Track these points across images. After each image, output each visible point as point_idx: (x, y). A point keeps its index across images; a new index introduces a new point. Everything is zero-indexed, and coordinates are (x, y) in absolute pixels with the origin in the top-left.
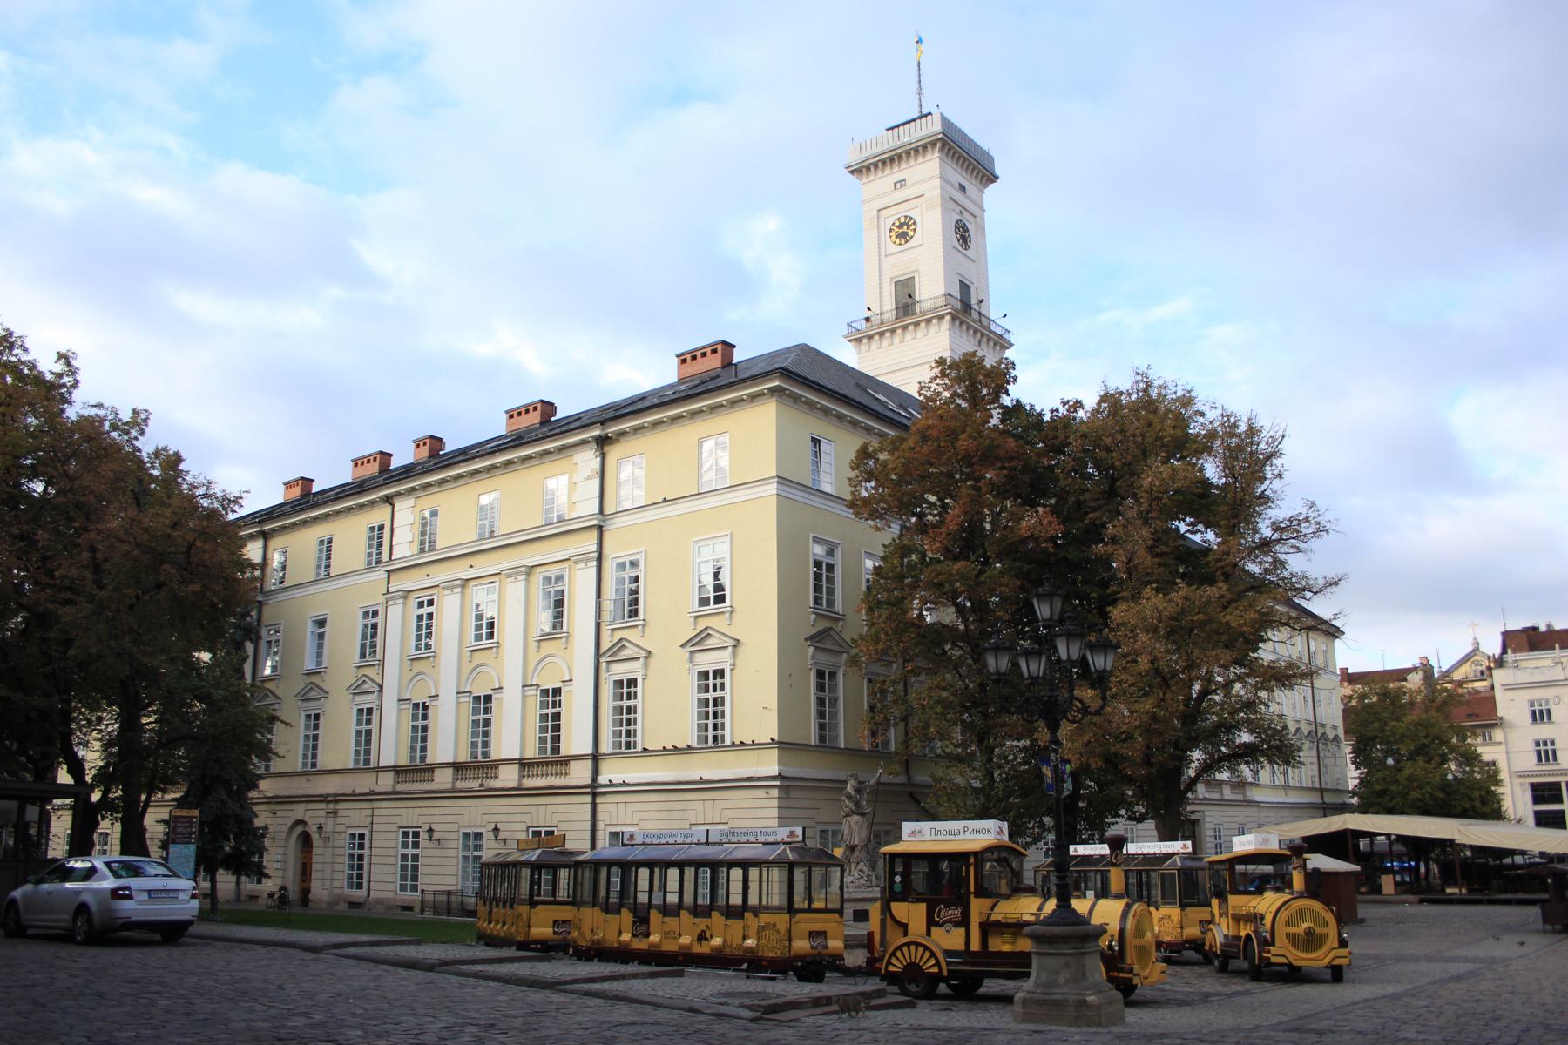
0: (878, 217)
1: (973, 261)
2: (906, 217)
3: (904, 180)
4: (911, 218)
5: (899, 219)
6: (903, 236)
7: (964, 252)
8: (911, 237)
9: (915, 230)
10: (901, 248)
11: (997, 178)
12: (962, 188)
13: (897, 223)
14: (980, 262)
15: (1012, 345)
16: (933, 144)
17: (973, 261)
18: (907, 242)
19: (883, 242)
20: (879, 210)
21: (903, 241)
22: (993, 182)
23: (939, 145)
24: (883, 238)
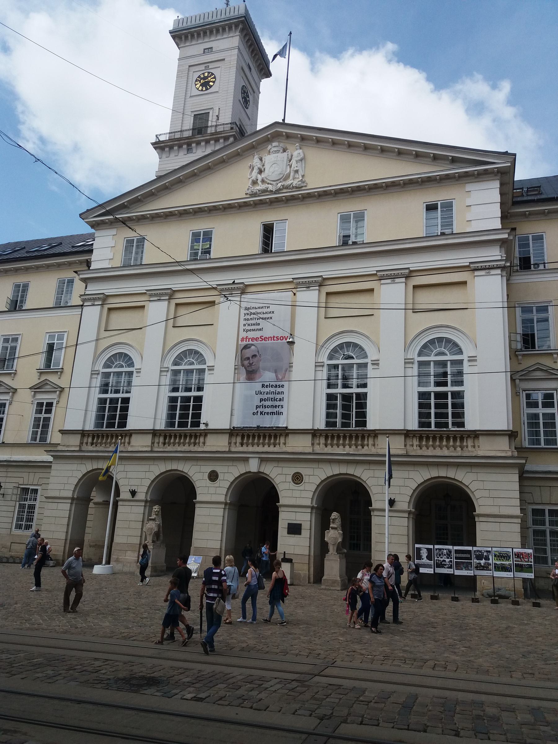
0: (189, 69)
1: (249, 119)
2: (209, 73)
3: (212, 48)
4: (213, 74)
5: (203, 74)
6: (206, 85)
7: (245, 109)
8: (211, 86)
9: (214, 82)
12: (250, 68)
13: (202, 76)
17: (249, 119)
18: (207, 89)
19: (189, 87)
20: (190, 66)
21: (204, 89)
24: (190, 85)
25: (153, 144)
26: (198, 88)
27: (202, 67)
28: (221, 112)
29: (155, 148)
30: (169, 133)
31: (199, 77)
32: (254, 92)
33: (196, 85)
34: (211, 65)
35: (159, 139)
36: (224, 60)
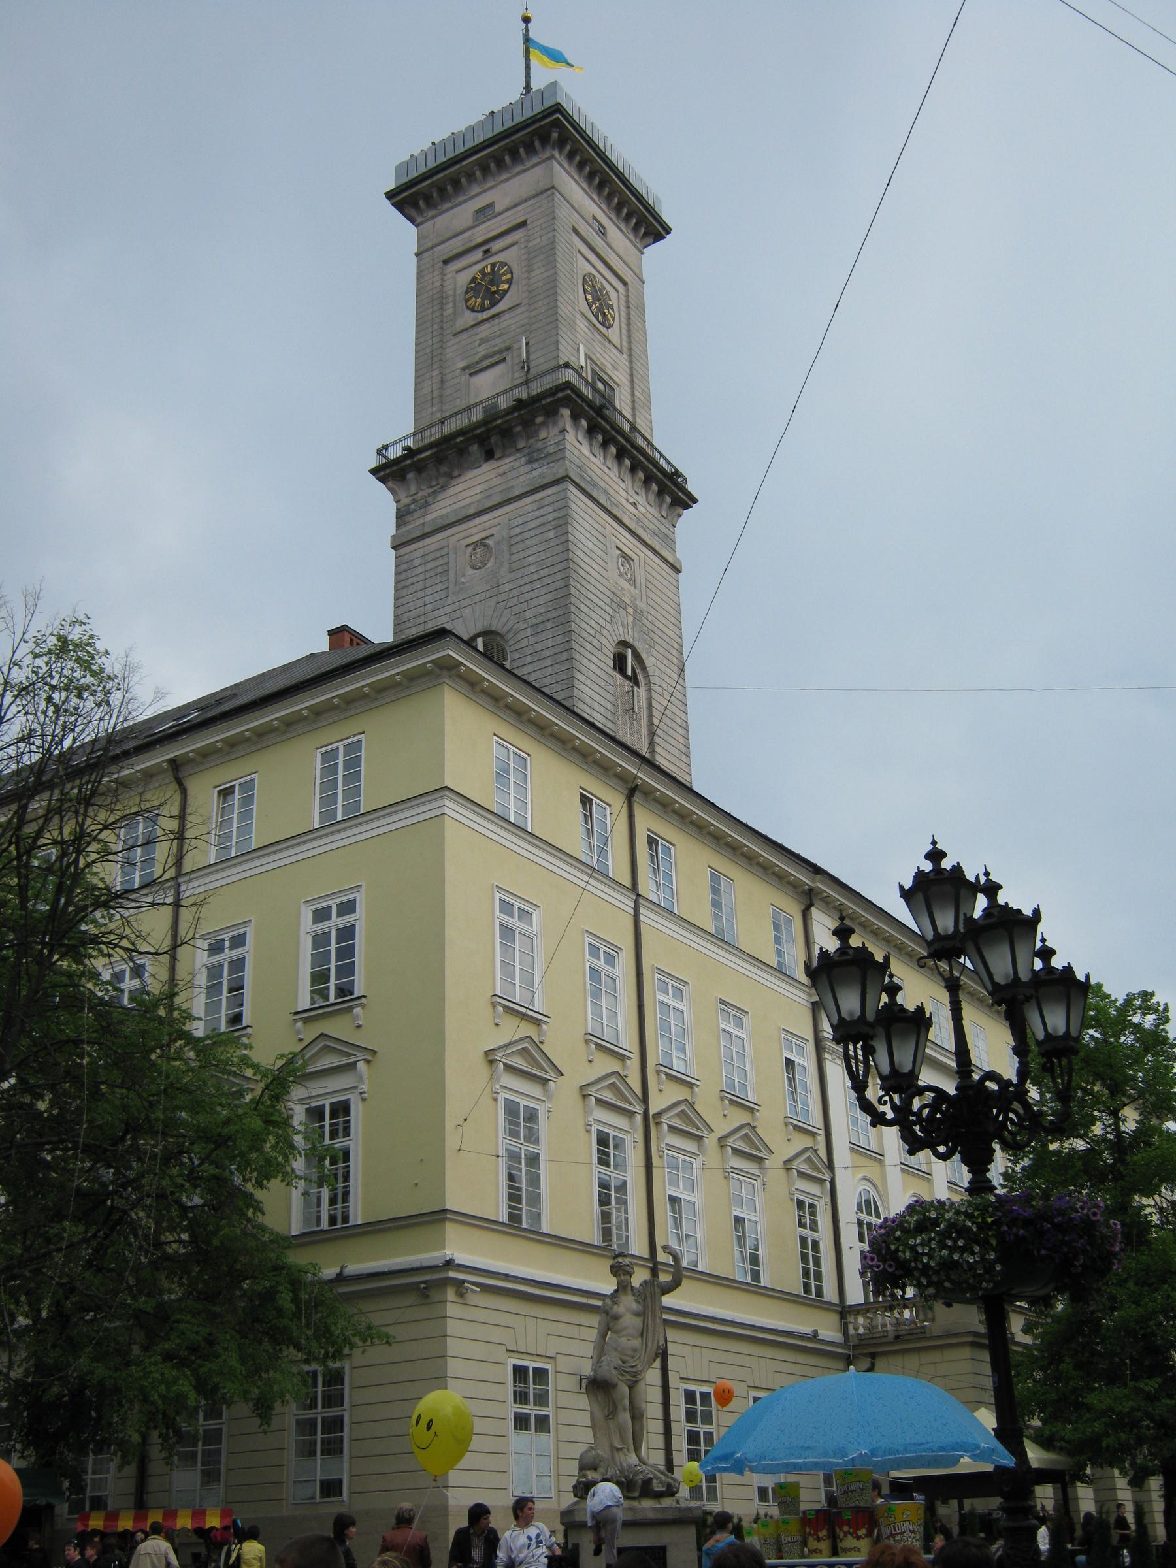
2: (493, 265)
3: (491, 206)
4: (503, 264)
5: (482, 271)
9: (510, 282)
10: (485, 315)
11: (668, 230)
14: (633, 350)
15: (695, 501)
16: (545, 140)
17: (621, 352)
18: (493, 305)
20: (446, 262)
21: (487, 303)
22: (658, 237)
23: (555, 135)
25: (374, 472)
26: (474, 307)
27: (478, 254)
28: (532, 350)
29: (382, 480)
30: (414, 434)
31: (473, 280)
32: (625, 283)
33: (467, 301)
34: (496, 246)
35: (386, 458)
36: (524, 224)
